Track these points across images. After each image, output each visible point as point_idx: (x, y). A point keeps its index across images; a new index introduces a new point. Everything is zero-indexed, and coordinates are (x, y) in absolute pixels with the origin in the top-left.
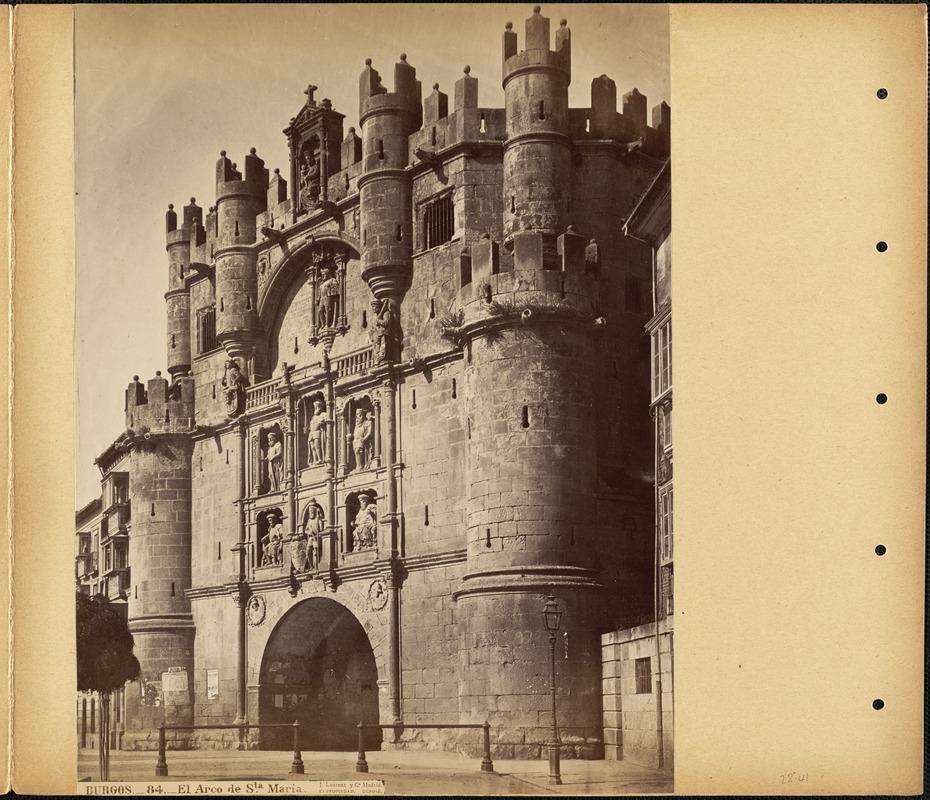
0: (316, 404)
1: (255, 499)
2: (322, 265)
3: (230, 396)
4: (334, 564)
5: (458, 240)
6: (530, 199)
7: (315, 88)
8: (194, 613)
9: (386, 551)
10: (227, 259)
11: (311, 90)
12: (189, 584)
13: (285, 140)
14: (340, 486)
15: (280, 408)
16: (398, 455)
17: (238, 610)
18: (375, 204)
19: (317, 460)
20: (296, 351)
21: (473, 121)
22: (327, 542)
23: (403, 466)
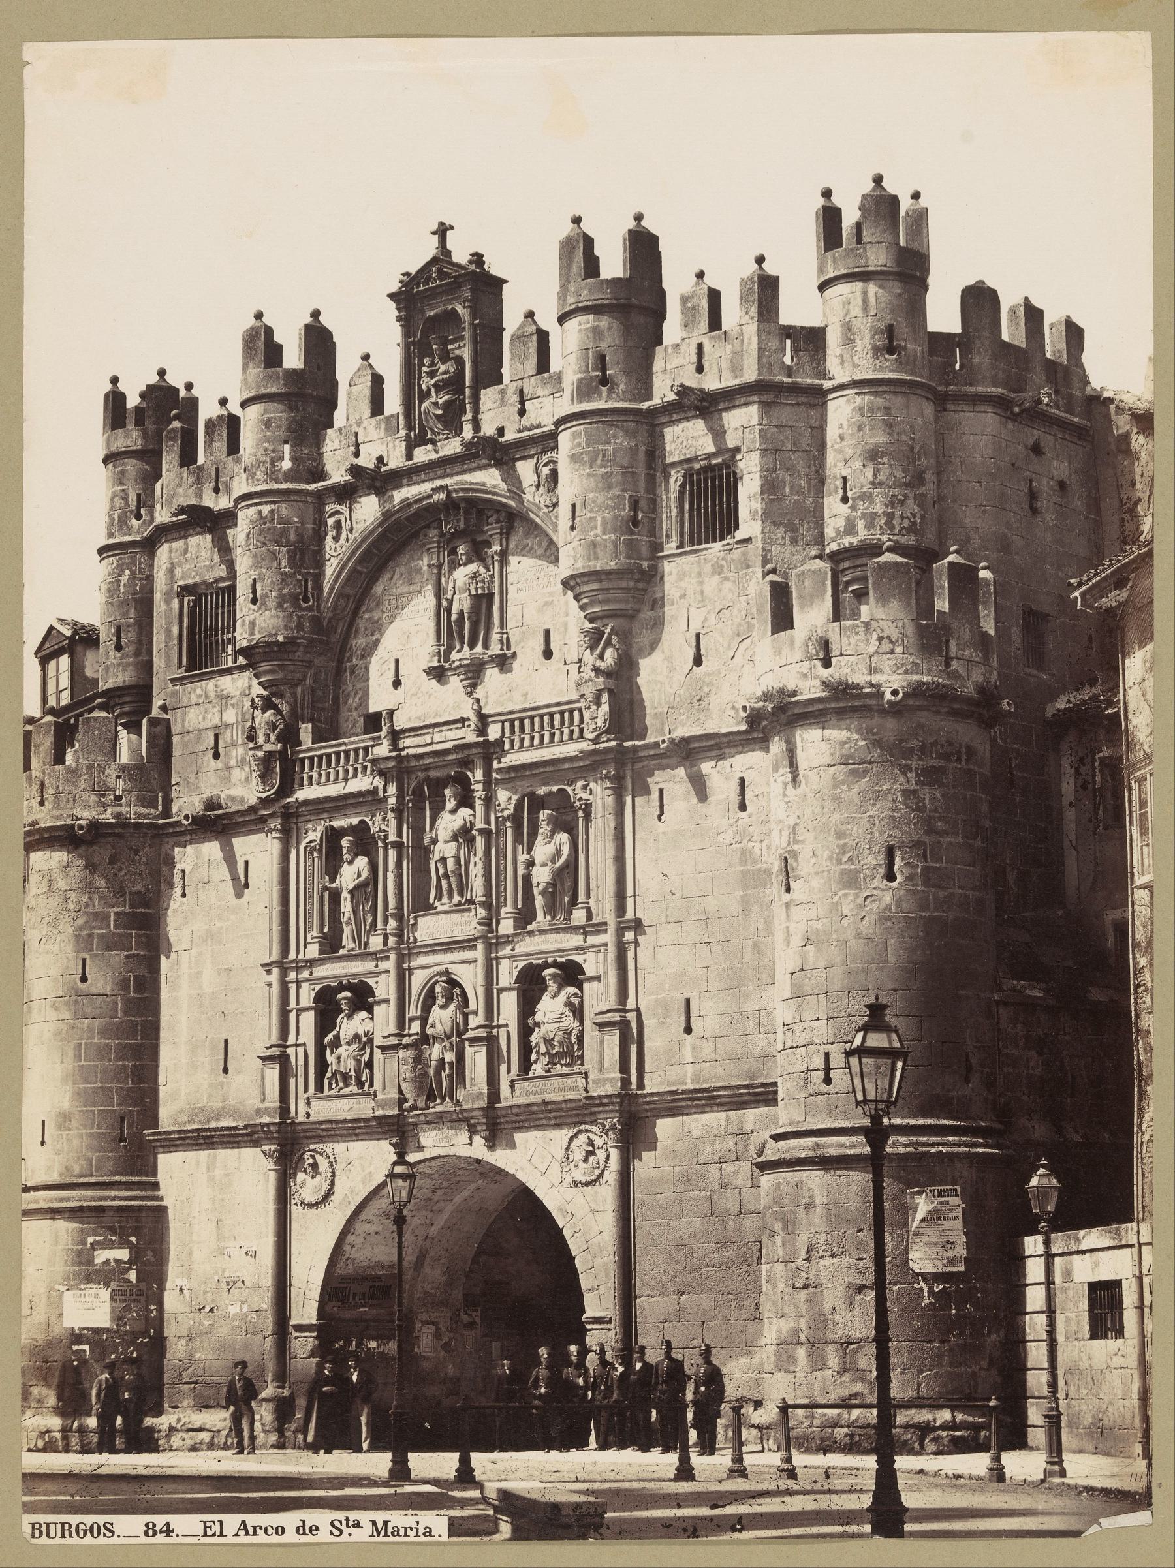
1: (311, 963)
2: (458, 535)
3: (266, 764)
4: (494, 1095)
7: (452, 228)
8: (161, 1177)
10: (266, 509)
11: (442, 231)
12: (154, 1121)
13: (391, 309)
16: (630, 902)
17: (273, 1176)
19: (451, 897)
20: (397, 683)
21: (774, 344)
22: (477, 1058)
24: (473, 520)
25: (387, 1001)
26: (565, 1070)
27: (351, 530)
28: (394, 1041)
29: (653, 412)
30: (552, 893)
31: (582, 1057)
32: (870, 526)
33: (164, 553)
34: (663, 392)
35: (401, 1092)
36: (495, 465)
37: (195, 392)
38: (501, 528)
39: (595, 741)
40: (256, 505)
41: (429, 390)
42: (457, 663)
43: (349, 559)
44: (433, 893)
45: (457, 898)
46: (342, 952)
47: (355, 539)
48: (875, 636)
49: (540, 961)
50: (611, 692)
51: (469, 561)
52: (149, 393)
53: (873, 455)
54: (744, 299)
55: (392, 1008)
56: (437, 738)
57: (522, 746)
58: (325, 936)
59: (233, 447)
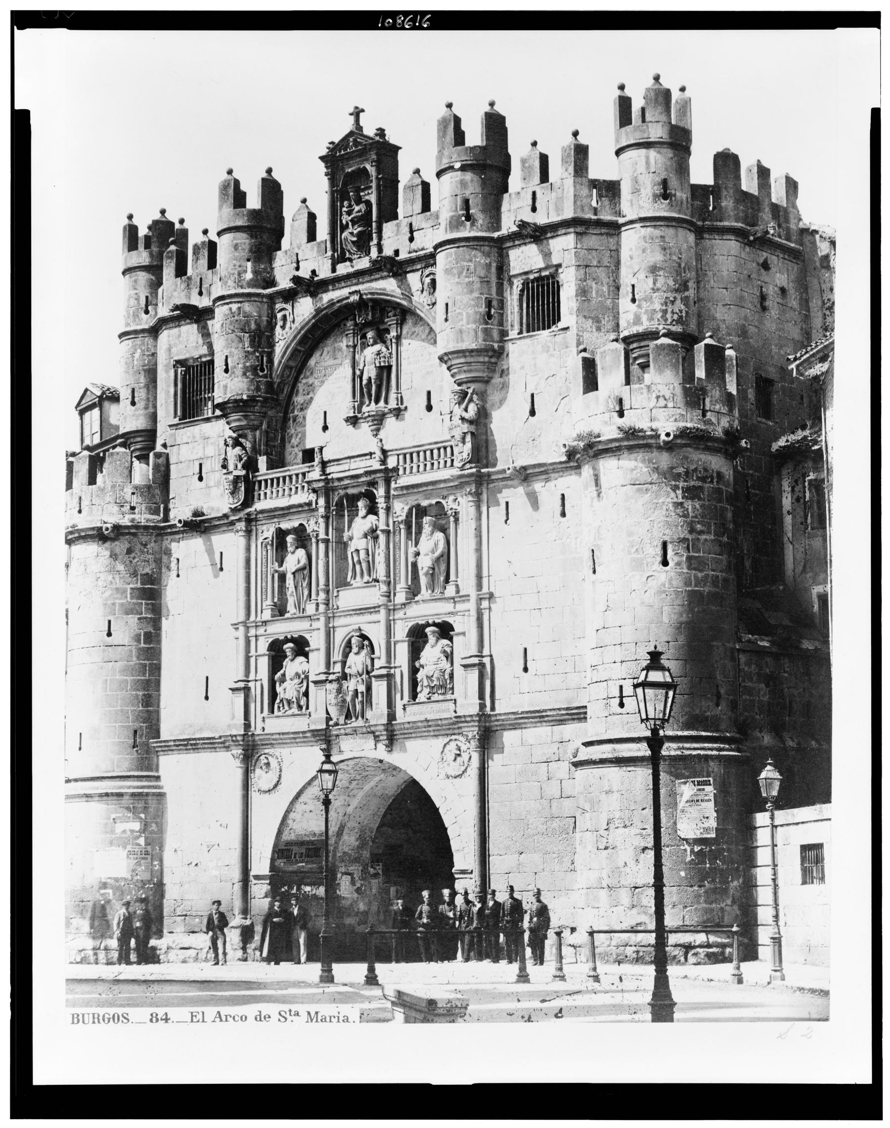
0: (361, 504)
1: (265, 623)
2: (368, 325)
4: (392, 716)
5: (567, 328)
6: (654, 290)
7: (363, 111)
8: (161, 773)
9: (469, 705)
10: (235, 307)
11: (357, 113)
12: (157, 734)
13: (321, 167)
14: (399, 614)
15: (309, 504)
16: (485, 581)
17: (239, 774)
18: (460, 274)
20: (325, 428)
21: (585, 191)
22: (380, 689)
23: (491, 596)
24: (378, 315)
25: (318, 649)
26: (441, 698)
27: (293, 322)
28: (323, 677)
29: (502, 240)
30: (432, 575)
31: (452, 688)
32: (651, 319)
33: (165, 336)
34: (508, 225)
35: (328, 713)
36: (393, 276)
37: (186, 225)
38: (397, 320)
39: (462, 468)
40: (228, 304)
41: (347, 223)
42: (367, 414)
43: (292, 341)
44: (350, 574)
45: (366, 578)
46: (287, 615)
47: (296, 328)
48: (654, 395)
49: (423, 622)
50: (472, 434)
51: (375, 343)
52: (155, 226)
53: (654, 270)
54: (564, 161)
55: (322, 655)
56: (353, 466)
57: (411, 472)
58: (275, 605)
59: (212, 263)
